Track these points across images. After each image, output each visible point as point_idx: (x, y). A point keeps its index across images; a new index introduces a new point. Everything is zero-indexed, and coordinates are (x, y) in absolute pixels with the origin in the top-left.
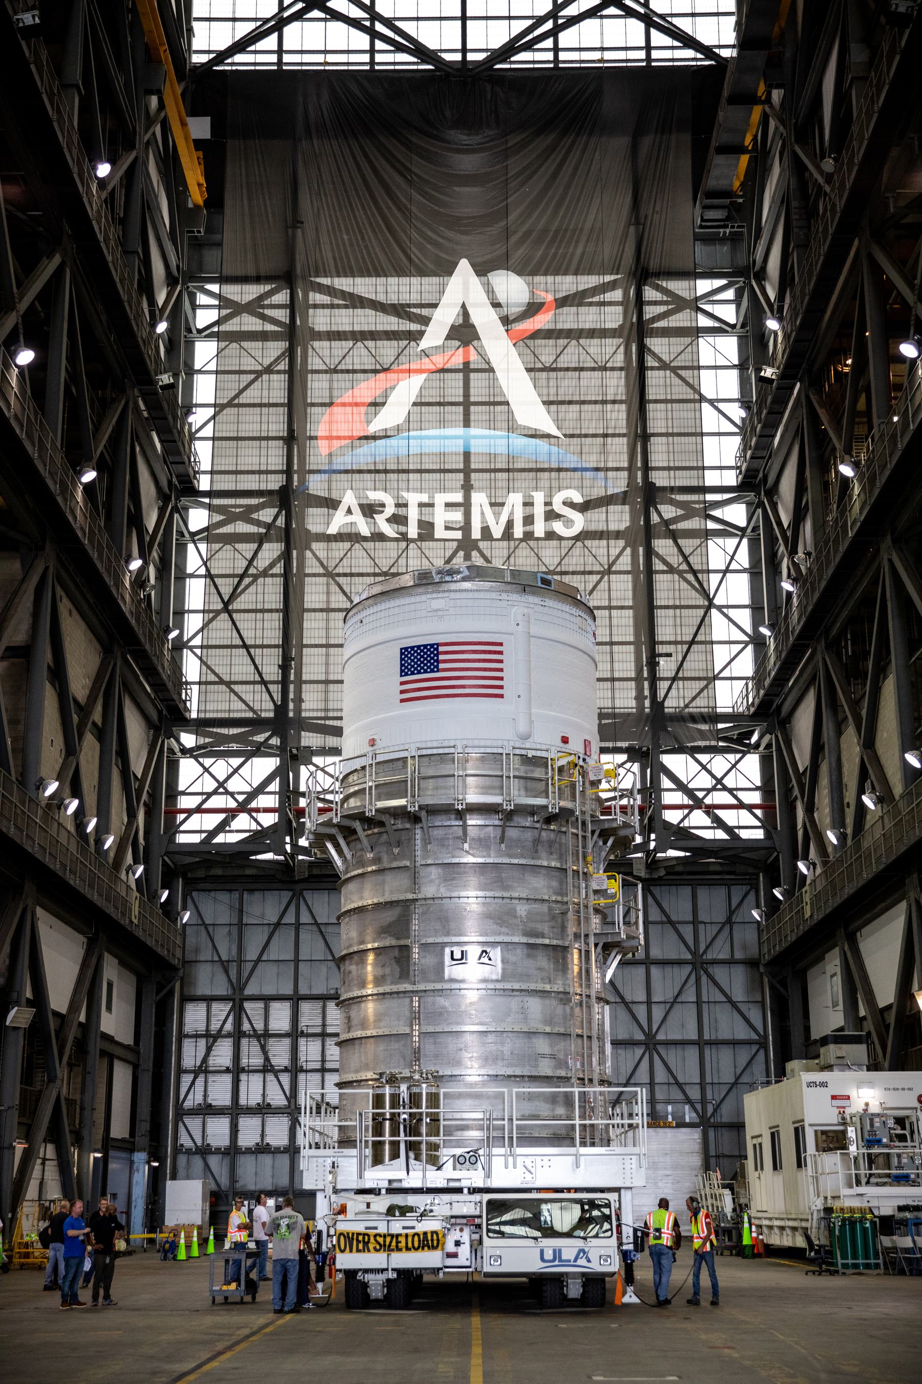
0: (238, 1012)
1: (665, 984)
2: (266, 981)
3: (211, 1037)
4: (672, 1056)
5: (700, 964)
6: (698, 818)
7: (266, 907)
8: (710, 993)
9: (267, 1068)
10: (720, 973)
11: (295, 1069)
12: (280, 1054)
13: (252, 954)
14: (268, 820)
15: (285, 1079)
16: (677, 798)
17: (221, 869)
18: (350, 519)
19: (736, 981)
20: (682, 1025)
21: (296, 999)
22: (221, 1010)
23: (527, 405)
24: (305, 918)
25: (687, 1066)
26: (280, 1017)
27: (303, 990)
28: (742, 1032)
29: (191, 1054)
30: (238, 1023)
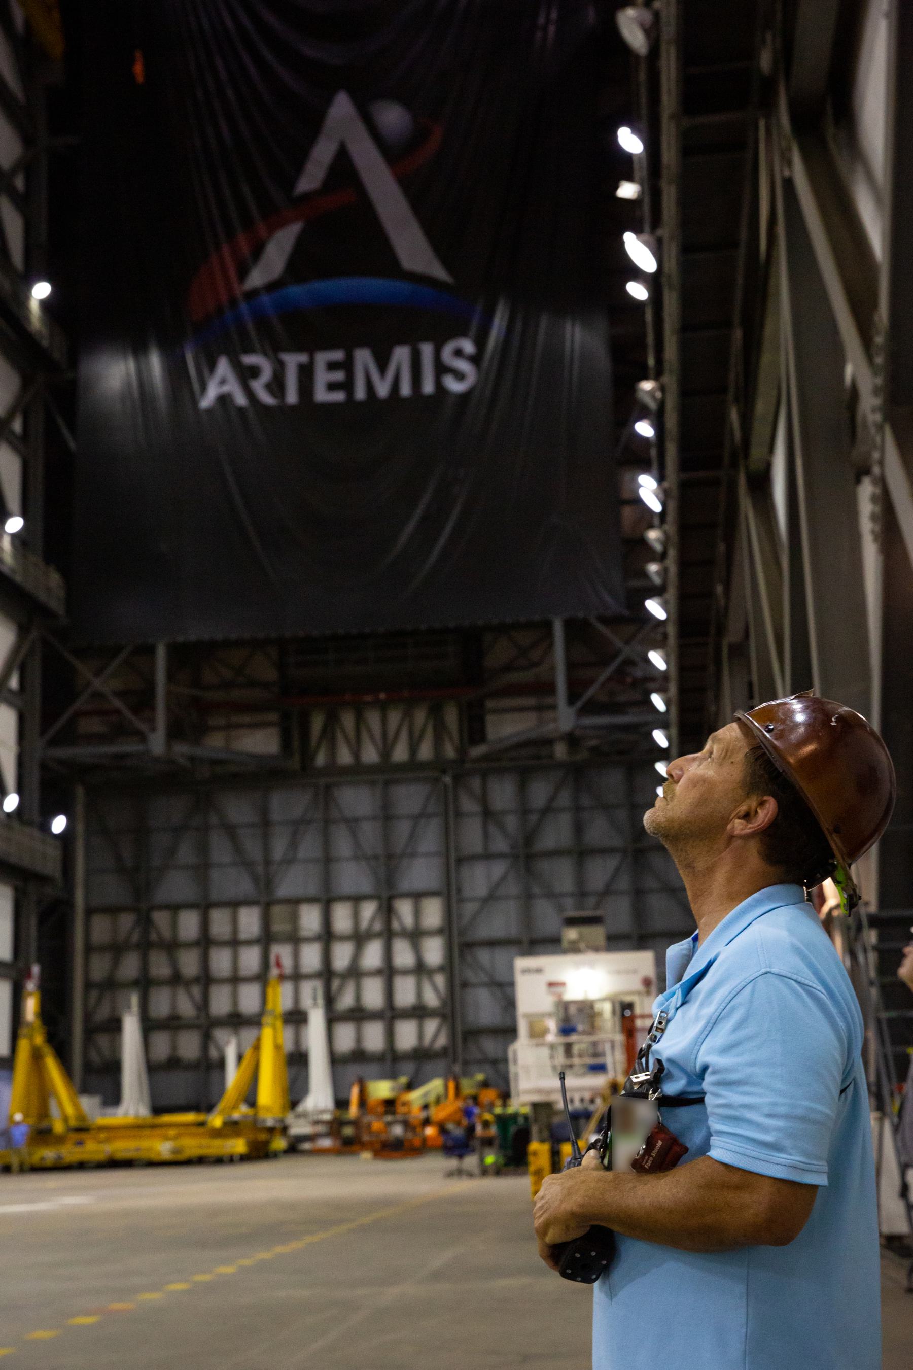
0: (145, 922)
3: (117, 950)
9: (176, 980)
11: (206, 980)
12: (189, 963)
15: (196, 991)
18: (226, 389)
21: (205, 907)
22: (127, 921)
23: (413, 249)
24: (214, 820)
26: (189, 925)
27: (214, 896)
30: (146, 932)
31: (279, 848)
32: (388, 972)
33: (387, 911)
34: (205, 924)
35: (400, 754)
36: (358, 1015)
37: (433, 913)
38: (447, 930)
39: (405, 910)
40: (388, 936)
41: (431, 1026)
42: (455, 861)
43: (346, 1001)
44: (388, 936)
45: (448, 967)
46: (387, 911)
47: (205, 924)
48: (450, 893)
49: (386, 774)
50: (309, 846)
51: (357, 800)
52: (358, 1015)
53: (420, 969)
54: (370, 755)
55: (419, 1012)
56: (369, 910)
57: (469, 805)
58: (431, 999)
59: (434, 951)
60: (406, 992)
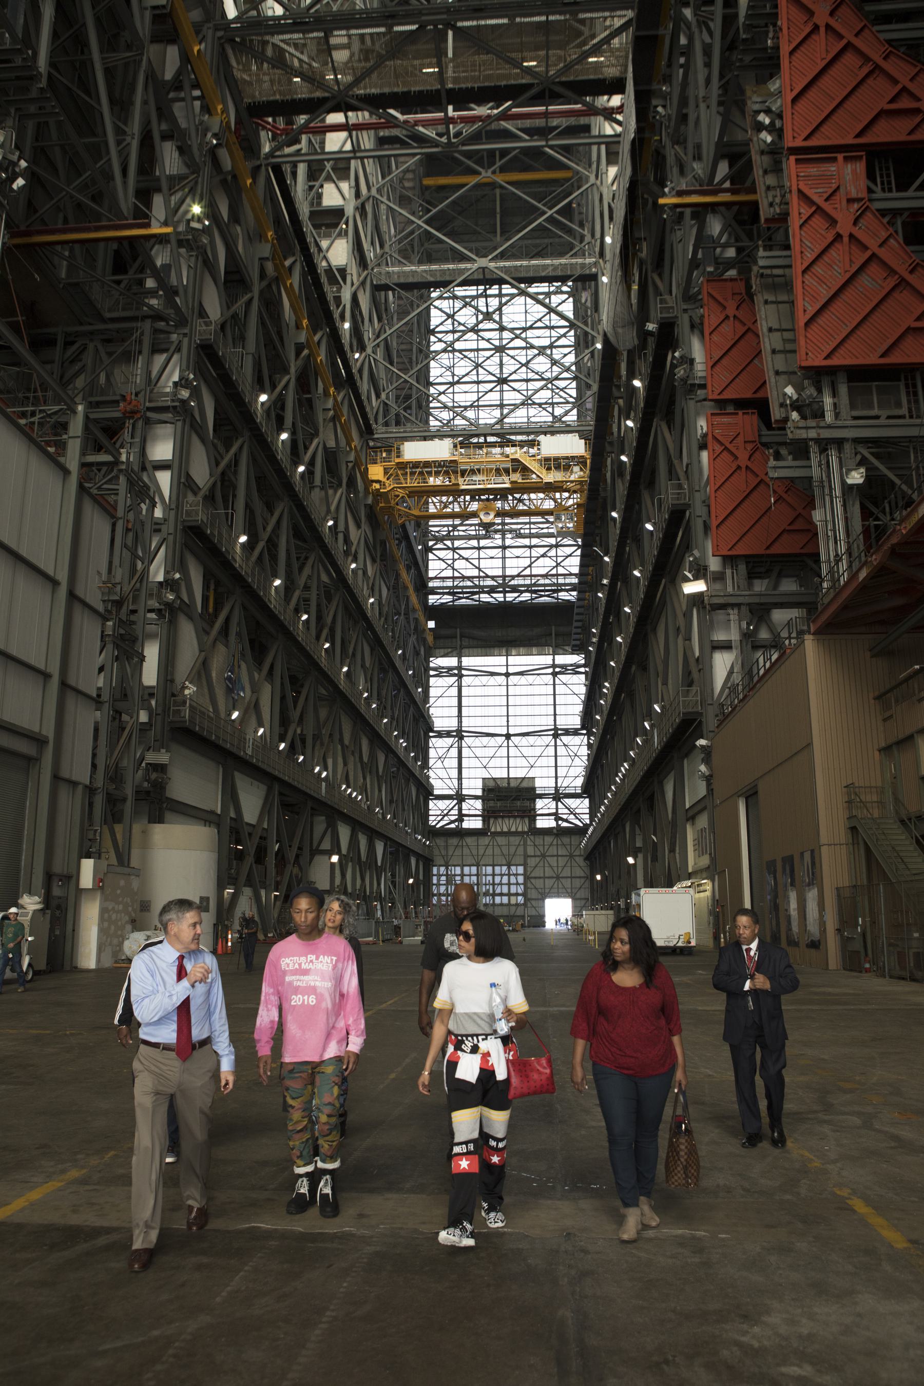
1: (562, 861)
2: (454, 860)
4: (563, 881)
5: (571, 856)
6: (572, 816)
7: (454, 841)
8: (574, 864)
10: (577, 859)
13: (450, 853)
14: (453, 818)
16: (566, 811)
17: (444, 833)
19: (580, 861)
20: (567, 872)
25: (567, 883)
28: (582, 874)
29: (435, 880)
31: (481, 852)
32: (509, 884)
33: (509, 868)
34: (462, 870)
35: (513, 829)
36: (501, 894)
37: (521, 870)
38: (525, 874)
39: (513, 868)
40: (509, 875)
41: (520, 898)
42: (526, 856)
43: (498, 891)
44: (509, 875)
45: (525, 884)
46: (509, 868)
47: (462, 870)
48: (525, 865)
49: (509, 834)
50: (489, 851)
51: (501, 840)
52: (501, 894)
53: (517, 884)
54: (505, 829)
55: (517, 894)
56: (504, 868)
57: (529, 842)
58: (520, 891)
59: (521, 879)
60: (513, 889)
